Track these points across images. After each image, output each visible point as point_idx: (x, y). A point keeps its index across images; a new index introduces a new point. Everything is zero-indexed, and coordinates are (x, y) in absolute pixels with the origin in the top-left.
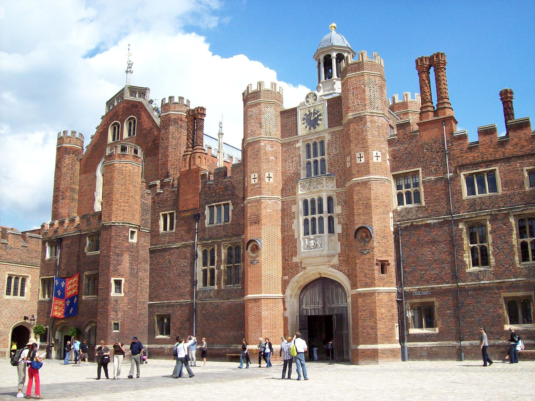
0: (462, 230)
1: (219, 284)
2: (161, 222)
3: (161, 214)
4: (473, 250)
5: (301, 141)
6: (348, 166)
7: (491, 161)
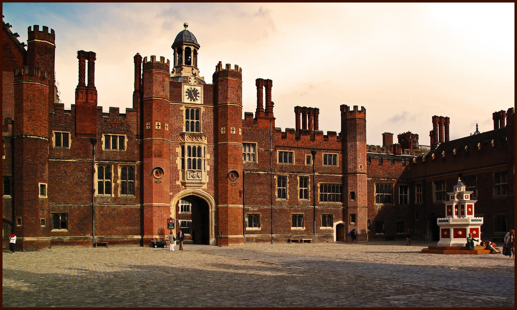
0: (275, 179)
1: (116, 193)
2: (54, 139)
3: (53, 132)
4: (279, 190)
5: (184, 106)
6: (222, 132)
7: (291, 147)
